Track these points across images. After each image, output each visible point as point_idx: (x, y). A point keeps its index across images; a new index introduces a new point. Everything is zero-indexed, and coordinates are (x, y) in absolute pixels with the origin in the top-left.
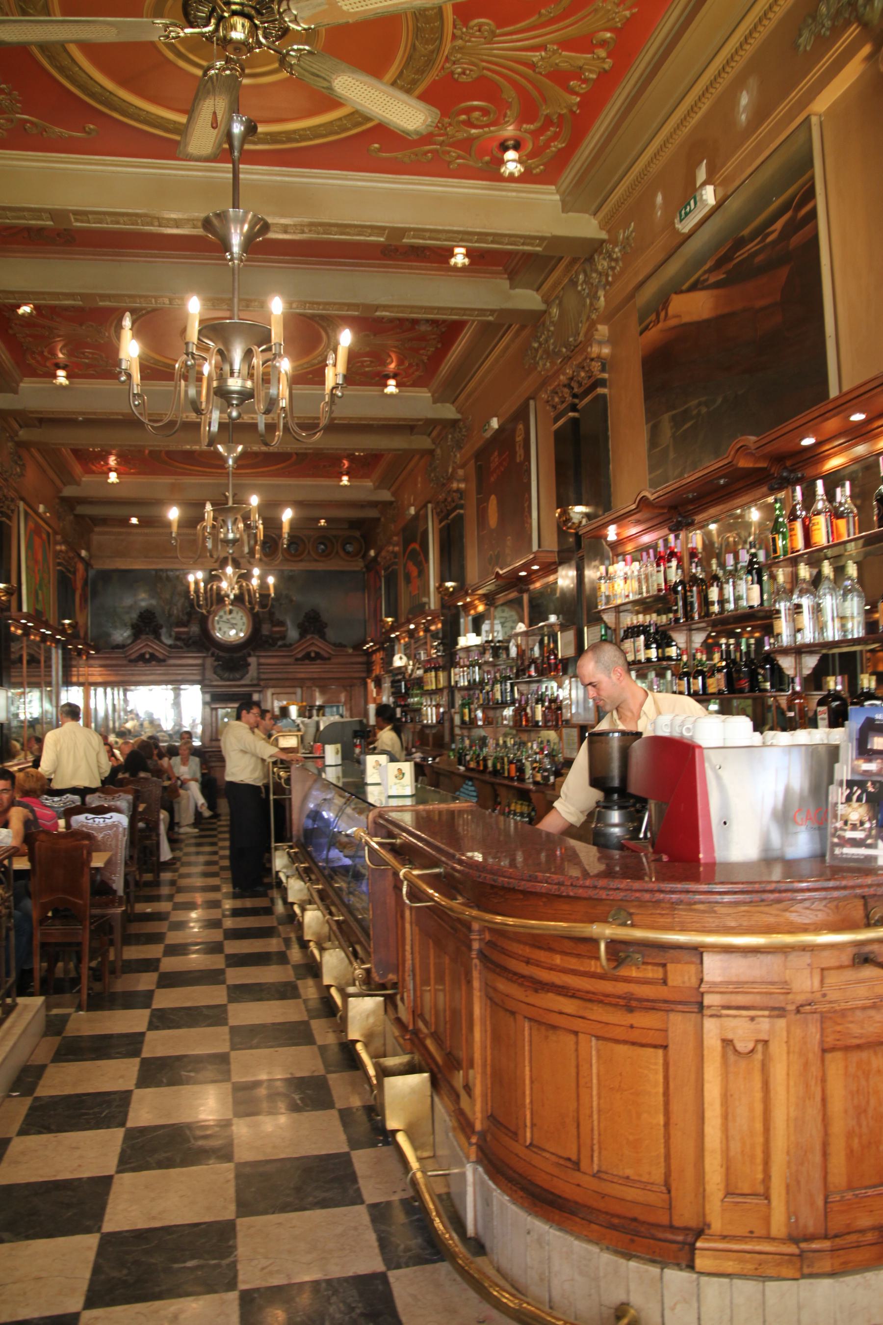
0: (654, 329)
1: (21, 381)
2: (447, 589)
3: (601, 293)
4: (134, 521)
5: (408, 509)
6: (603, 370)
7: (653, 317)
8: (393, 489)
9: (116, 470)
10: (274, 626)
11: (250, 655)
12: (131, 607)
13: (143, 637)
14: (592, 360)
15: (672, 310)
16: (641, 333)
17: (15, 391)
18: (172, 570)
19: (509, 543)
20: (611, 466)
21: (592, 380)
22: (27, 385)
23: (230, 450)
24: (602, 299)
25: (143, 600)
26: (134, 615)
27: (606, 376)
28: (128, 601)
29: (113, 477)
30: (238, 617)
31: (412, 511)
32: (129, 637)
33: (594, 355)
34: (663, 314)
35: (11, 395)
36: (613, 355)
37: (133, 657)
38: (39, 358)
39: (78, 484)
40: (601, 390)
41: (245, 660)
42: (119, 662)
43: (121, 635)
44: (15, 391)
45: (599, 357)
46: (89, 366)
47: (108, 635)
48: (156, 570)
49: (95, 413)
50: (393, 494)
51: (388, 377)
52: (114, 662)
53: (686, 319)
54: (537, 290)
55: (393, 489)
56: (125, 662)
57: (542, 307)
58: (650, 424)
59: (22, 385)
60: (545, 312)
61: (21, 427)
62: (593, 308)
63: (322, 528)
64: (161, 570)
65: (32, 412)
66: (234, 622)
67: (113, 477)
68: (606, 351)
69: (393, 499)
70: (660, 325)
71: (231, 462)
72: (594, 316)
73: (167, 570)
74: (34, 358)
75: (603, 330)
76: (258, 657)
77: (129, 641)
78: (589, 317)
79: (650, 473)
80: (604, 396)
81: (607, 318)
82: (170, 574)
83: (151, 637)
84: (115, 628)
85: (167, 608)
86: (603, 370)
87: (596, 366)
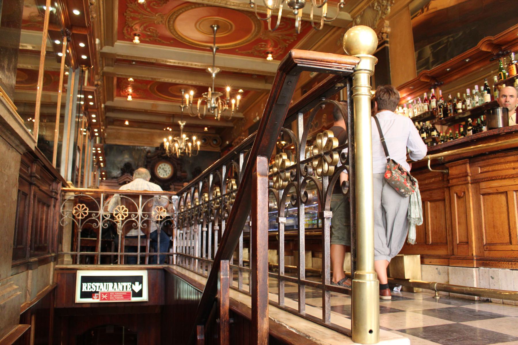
0: (420, 16)
1: (116, 42)
2: (282, 144)
3: (389, 8)
4: (127, 123)
5: (255, 117)
6: (387, 37)
7: (420, 11)
8: (244, 113)
9: (131, 95)
10: (182, 173)
11: (171, 184)
12: (121, 161)
13: (126, 174)
14: (383, 33)
15: (430, 7)
16: (412, 19)
17: (113, 46)
18: (139, 146)
19: (324, 117)
20: (391, 74)
21: (382, 41)
22: (119, 43)
23: (213, 71)
24: (389, 10)
25: (126, 158)
26: (122, 165)
27: (388, 40)
28: (120, 159)
29: (130, 98)
30: (168, 168)
31: (258, 118)
32: (119, 174)
33: (384, 31)
34: (425, 9)
35: (110, 47)
36: (391, 32)
37: (121, 182)
38: (129, 30)
39: (113, 100)
40: (386, 45)
41: (169, 186)
42: (115, 184)
43: (116, 173)
44: (113, 46)
45: (386, 33)
46: (149, 36)
47: (111, 172)
48: (133, 146)
49: (145, 58)
50: (244, 115)
51: (268, 53)
52: (112, 184)
53: (439, 8)
54: (349, 13)
55: (244, 113)
56: (117, 185)
57: (351, 19)
58: (417, 52)
59: (116, 43)
60: (352, 22)
61: (106, 66)
62: (384, 13)
63: (206, 132)
64: (135, 146)
65: (118, 55)
66: (165, 169)
67: (130, 98)
68: (389, 30)
69: (243, 117)
70: (424, 14)
71: (214, 75)
72: (384, 17)
73: (137, 146)
74: (127, 30)
75: (387, 22)
76: (175, 185)
77: (119, 176)
78: (381, 18)
79: (417, 70)
80: (387, 47)
81: (389, 18)
82: (138, 148)
83: (129, 174)
84: (114, 169)
85: (136, 162)
86: (387, 37)
87: (385, 36)
